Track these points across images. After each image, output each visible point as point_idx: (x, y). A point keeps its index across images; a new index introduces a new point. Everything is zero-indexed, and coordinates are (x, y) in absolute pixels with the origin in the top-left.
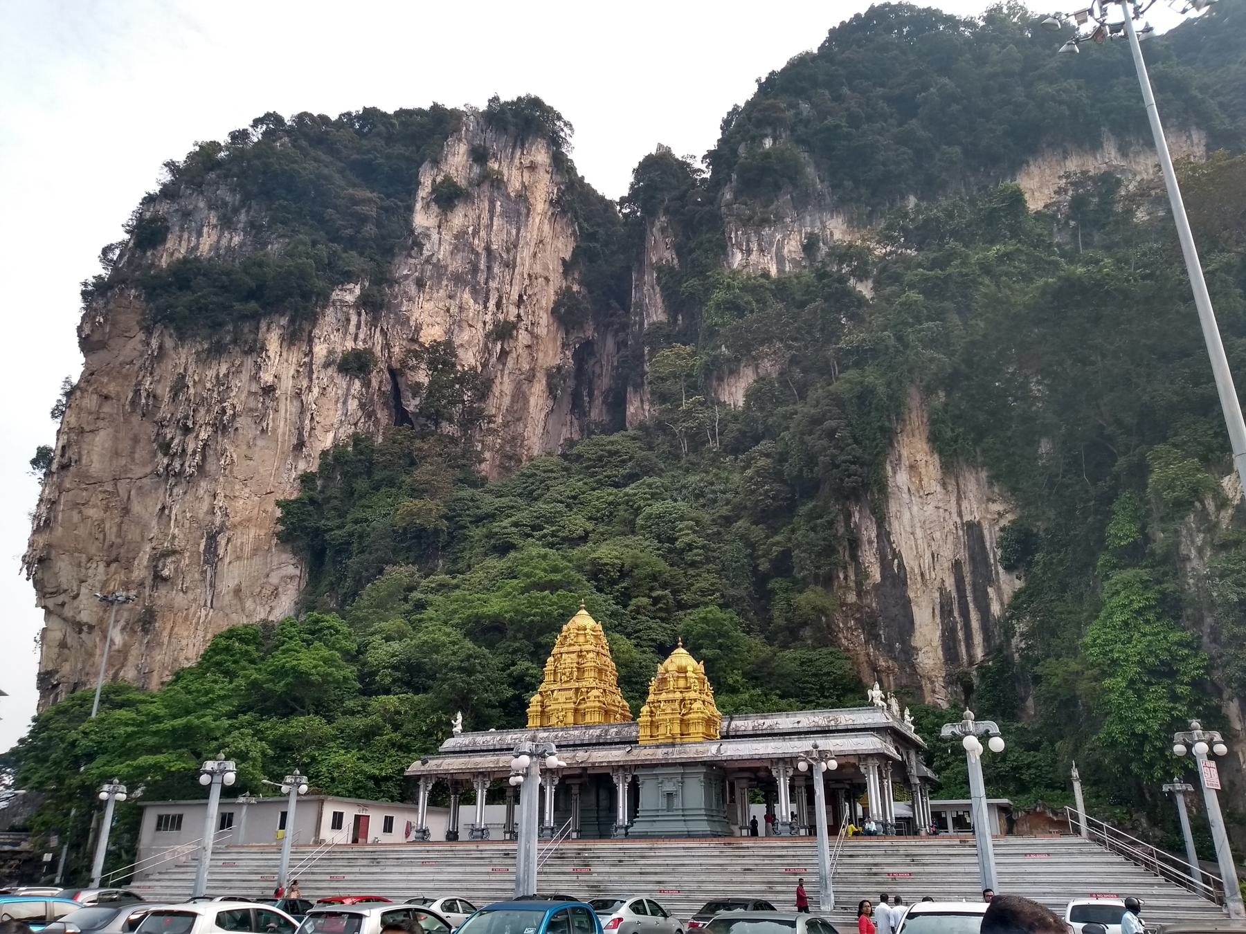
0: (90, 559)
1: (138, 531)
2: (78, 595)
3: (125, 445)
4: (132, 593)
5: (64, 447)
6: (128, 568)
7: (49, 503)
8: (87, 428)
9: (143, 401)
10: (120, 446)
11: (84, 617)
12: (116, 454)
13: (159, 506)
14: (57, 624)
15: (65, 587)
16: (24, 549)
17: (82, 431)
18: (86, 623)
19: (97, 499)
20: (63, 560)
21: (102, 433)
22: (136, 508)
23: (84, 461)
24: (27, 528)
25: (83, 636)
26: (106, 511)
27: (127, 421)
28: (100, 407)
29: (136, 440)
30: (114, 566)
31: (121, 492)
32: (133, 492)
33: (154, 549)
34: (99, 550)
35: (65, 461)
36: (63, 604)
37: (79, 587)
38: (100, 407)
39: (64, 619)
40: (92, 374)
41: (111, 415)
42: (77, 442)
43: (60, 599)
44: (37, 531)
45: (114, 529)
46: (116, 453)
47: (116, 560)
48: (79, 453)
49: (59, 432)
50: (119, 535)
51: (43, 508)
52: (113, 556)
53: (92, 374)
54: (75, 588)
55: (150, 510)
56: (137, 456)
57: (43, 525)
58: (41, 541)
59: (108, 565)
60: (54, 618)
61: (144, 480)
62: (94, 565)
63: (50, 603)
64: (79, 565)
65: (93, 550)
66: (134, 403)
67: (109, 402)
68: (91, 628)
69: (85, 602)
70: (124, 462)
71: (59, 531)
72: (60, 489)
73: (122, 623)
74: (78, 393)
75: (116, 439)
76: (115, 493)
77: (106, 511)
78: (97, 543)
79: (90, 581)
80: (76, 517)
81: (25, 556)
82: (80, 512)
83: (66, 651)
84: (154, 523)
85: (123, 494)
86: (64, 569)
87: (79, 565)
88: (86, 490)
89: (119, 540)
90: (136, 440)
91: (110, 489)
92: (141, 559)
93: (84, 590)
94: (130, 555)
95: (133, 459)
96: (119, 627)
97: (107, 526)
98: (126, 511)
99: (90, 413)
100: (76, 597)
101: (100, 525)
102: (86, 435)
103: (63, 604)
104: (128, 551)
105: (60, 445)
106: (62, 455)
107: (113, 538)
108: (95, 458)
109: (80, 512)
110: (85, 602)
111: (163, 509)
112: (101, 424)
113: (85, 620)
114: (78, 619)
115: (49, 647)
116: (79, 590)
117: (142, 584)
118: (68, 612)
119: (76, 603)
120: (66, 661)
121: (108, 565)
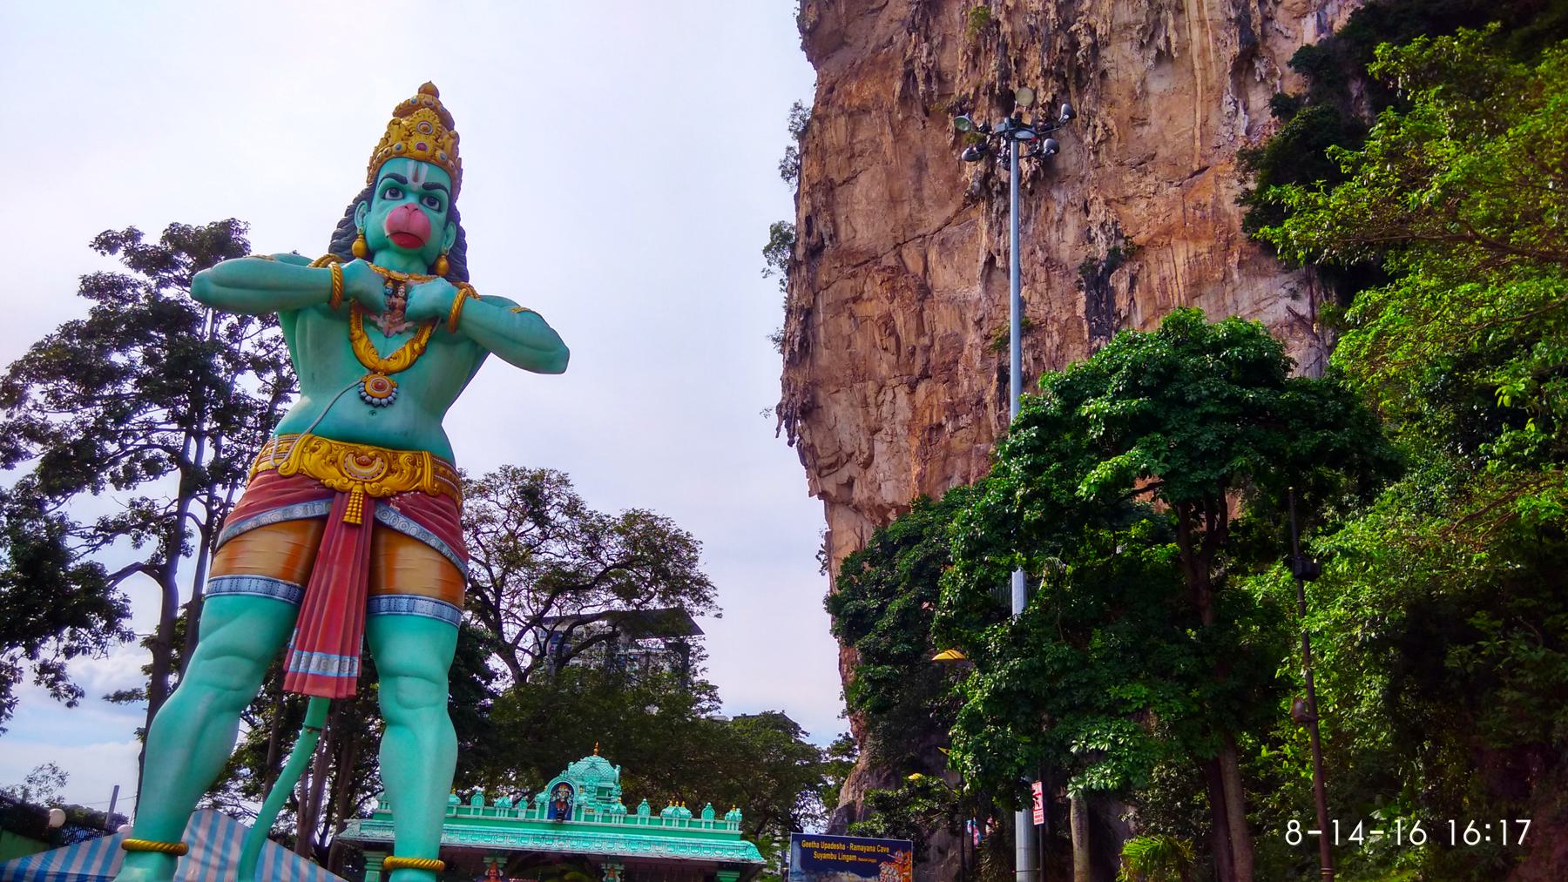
2: (871, 457)
3: (906, 183)
4: (965, 420)
5: (808, 220)
6: (952, 381)
7: (802, 315)
8: (838, 180)
9: (922, 87)
10: (896, 187)
12: (894, 201)
13: (983, 258)
14: (845, 518)
15: (848, 449)
16: (776, 395)
17: (829, 187)
18: (894, 505)
19: (873, 286)
20: (837, 402)
21: (862, 178)
22: (943, 277)
23: (843, 236)
24: (773, 364)
26: (892, 300)
27: (899, 138)
29: (921, 166)
30: (922, 389)
32: (933, 256)
33: (987, 338)
35: (814, 240)
36: (850, 483)
37: (871, 443)
38: (853, 136)
39: (857, 509)
40: (831, 90)
41: (873, 141)
42: (829, 206)
43: (844, 474)
44: (790, 364)
45: (913, 324)
47: (925, 375)
48: (834, 222)
49: (797, 197)
50: (920, 332)
51: (794, 323)
52: (917, 371)
53: (831, 90)
54: (865, 447)
55: (967, 274)
56: (926, 192)
58: (800, 379)
59: (913, 389)
60: (840, 510)
61: (947, 230)
62: (889, 397)
63: (830, 485)
64: (865, 404)
66: (905, 98)
67: (866, 120)
69: (884, 466)
70: (907, 210)
71: (824, 357)
72: (813, 288)
75: (890, 175)
76: (900, 269)
77: (892, 300)
79: (886, 426)
80: (846, 325)
81: (779, 407)
82: (852, 315)
84: (978, 290)
85: (913, 263)
86: (841, 411)
87: (865, 404)
88: (854, 275)
89: (926, 341)
90: (921, 166)
91: (892, 262)
92: (969, 360)
93: (880, 447)
94: (949, 358)
95: (921, 201)
97: (899, 320)
98: (925, 291)
99: (839, 152)
100: (867, 464)
101: (887, 323)
102: (838, 191)
104: (943, 351)
105: (803, 215)
106: (809, 233)
107: (913, 338)
108: (859, 222)
109: (852, 315)
110: (884, 466)
111: (991, 261)
112: (859, 164)
114: (878, 501)
116: (872, 448)
118: (860, 493)
119: (871, 472)
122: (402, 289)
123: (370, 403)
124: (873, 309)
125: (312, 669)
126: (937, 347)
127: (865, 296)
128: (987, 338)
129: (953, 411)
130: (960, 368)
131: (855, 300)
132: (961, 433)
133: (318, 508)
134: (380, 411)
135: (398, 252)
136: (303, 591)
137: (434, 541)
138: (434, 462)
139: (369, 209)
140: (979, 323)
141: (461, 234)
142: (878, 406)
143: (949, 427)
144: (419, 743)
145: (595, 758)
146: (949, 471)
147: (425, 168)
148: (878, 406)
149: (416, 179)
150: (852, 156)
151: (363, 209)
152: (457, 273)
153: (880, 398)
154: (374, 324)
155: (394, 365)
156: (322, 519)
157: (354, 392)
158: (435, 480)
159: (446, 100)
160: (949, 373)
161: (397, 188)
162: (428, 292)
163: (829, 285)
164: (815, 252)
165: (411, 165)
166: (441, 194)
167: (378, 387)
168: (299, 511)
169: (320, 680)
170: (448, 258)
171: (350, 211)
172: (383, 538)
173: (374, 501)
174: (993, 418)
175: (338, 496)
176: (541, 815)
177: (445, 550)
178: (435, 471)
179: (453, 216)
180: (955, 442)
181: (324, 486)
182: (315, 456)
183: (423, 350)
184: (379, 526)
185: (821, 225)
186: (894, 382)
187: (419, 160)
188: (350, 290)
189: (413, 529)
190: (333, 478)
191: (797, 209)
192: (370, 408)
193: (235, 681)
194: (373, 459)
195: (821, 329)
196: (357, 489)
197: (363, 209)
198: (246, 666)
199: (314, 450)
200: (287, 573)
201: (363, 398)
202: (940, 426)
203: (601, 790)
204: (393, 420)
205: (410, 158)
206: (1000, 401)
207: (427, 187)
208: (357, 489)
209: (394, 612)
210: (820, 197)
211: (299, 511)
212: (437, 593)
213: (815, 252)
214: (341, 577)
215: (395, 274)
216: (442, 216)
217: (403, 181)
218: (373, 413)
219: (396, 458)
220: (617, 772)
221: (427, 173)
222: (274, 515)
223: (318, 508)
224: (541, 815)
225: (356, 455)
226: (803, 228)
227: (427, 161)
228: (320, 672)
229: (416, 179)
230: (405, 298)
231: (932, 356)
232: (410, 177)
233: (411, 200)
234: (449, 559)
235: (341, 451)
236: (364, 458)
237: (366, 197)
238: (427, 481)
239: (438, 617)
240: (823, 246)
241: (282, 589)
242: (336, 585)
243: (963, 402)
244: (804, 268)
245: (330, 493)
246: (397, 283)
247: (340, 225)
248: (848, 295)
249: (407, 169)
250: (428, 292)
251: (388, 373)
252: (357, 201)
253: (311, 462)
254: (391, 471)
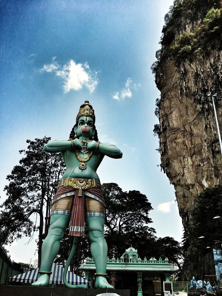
0: (184, 158)
1: (199, 139)
3: (184, 112)
4: (205, 163)
5: (162, 123)
8: (168, 114)
9: (185, 91)
10: (182, 113)
11: (189, 182)
12: (182, 116)
13: (204, 126)
14: (179, 188)
15: (178, 173)
16: (160, 162)
17: (167, 115)
18: (191, 184)
19: (179, 135)
21: (174, 112)
22: (195, 131)
23: (171, 125)
24: (159, 155)
25: (191, 190)
28: (170, 104)
29: (187, 108)
30: (194, 158)
31: (187, 129)
34: (186, 153)
35: (164, 127)
36: (179, 180)
39: (182, 186)
41: (175, 104)
42: (167, 119)
43: (178, 178)
44: (162, 155)
45: (190, 142)
46: (181, 116)
47: (194, 154)
49: (159, 119)
51: (162, 146)
52: (192, 153)
53: (164, 95)
54: (182, 171)
55: (201, 130)
56: (189, 113)
57: (164, 152)
62: (186, 159)
64: (181, 162)
65: (184, 154)
66: (181, 94)
68: (193, 186)
70: (185, 117)
71: (170, 153)
72: (165, 137)
73: (205, 177)
74: (162, 103)
75: (180, 111)
76: (185, 131)
78: (185, 151)
80: (174, 145)
81: (161, 165)
82: (175, 142)
83: (186, 199)
84: (204, 133)
87: (181, 162)
88: (174, 134)
89: (193, 146)
90: (187, 108)
92: (204, 149)
93: (185, 171)
95: (188, 115)
96: (205, 179)
97: (187, 142)
98: (192, 134)
100: (183, 176)
101: (184, 142)
103: (179, 180)
104: (198, 148)
105: (161, 122)
108: (174, 122)
109: (175, 142)
110: (187, 176)
111: (206, 127)
112: (172, 109)
113: (190, 183)
115: (179, 199)
116: (184, 172)
117: (208, 158)
118: (182, 182)
120: (187, 202)
121: (192, 157)
122: (85, 144)
123: (81, 169)
124: (180, 140)
125: (75, 230)
126: (196, 147)
127: (178, 138)
128: (208, 143)
129: (202, 161)
130: (203, 151)
131: (175, 139)
132: (204, 166)
133: (73, 193)
134: (83, 171)
135: (84, 136)
136: (71, 212)
137: (97, 199)
138: (95, 181)
139: (77, 128)
140: (205, 140)
141: (96, 131)
142: (184, 162)
143: (202, 165)
144: (100, 246)
145: (132, 248)
146: (203, 175)
147: (88, 118)
148: (184, 162)
149: (86, 120)
150: (171, 108)
151: (76, 128)
152: (96, 139)
153: (184, 160)
154: (81, 152)
155: (85, 160)
156: (73, 196)
157: (78, 167)
158: (96, 185)
159: (90, 104)
160: (200, 153)
161: (83, 123)
162: (92, 143)
163: (169, 136)
164: (165, 130)
165: (85, 117)
166: (92, 123)
167: (83, 165)
168: (69, 194)
169: (77, 232)
170: (94, 136)
171: (73, 129)
172: (87, 199)
173: (84, 191)
174: (212, 161)
175: (76, 190)
176: (122, 262)
177: (100, 201)
178: (96, 183)
179: (94, 127)
180: (204, 168)
181: (73, 188)
182: (71, 182)
183: (91, 157)
184: (86, 197)
185: (165, 124)
186: (187, 156)
187: (87, 116)
188: (75, 145)
189: (93, 196)
190: (75, 186)
191: (160, 121)
192: (82, 170)
193: (59, 234)
194: (83, 181)
195: (168, 146)
196: (80, 188)
197: (76, 128)
198: (61, 230)
199: (71, 181)
200: (67, 209)
201: (80, 168)
202: (200, 165)
203: (134, 255)
204: (87, 172)
205: (85, 116)
206: (213, 157)
207: (88, 121)
208: (80, 188)
209: (91, 216)
210: (165, 118)
211: (69, 194)
212: (99, 211)
213: (165, 130)
214: (79, 208)
215: (84, 141)
216: (92, 128)
217: (84, 121)
218: (82, 171)
219: (88, 181)
220: (137, 251)
221: (88, 119)
222: (64, 196)
223: (73, 193)
224: (122, 262)
225: (79, 181)
226: (161, 125)
227: (88, 116)
228: (76, 231)
229: (86, 120)
230: (86, 146)
231: (195, 149)
232: (85, 120)
233: (86, 125)
234: (101, 203)
235: (76, 179)
236: (81, 181)
237: (76, 125)
238: (95, 185)
239: (100, 216)
240: (167, 128)
241: (67, 212)
242: (78, 210)
243: (204, 159)
244: (163, 134)
245: (75, 190)
246: (84, 143)
247: (71, 132)
248: (173, 138)
249: (84, 118)
250: (92, 143)
251: (84, 162)
252: (74, 127)
253: (70, 183)
254: (87, 184)
